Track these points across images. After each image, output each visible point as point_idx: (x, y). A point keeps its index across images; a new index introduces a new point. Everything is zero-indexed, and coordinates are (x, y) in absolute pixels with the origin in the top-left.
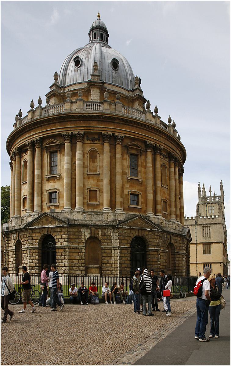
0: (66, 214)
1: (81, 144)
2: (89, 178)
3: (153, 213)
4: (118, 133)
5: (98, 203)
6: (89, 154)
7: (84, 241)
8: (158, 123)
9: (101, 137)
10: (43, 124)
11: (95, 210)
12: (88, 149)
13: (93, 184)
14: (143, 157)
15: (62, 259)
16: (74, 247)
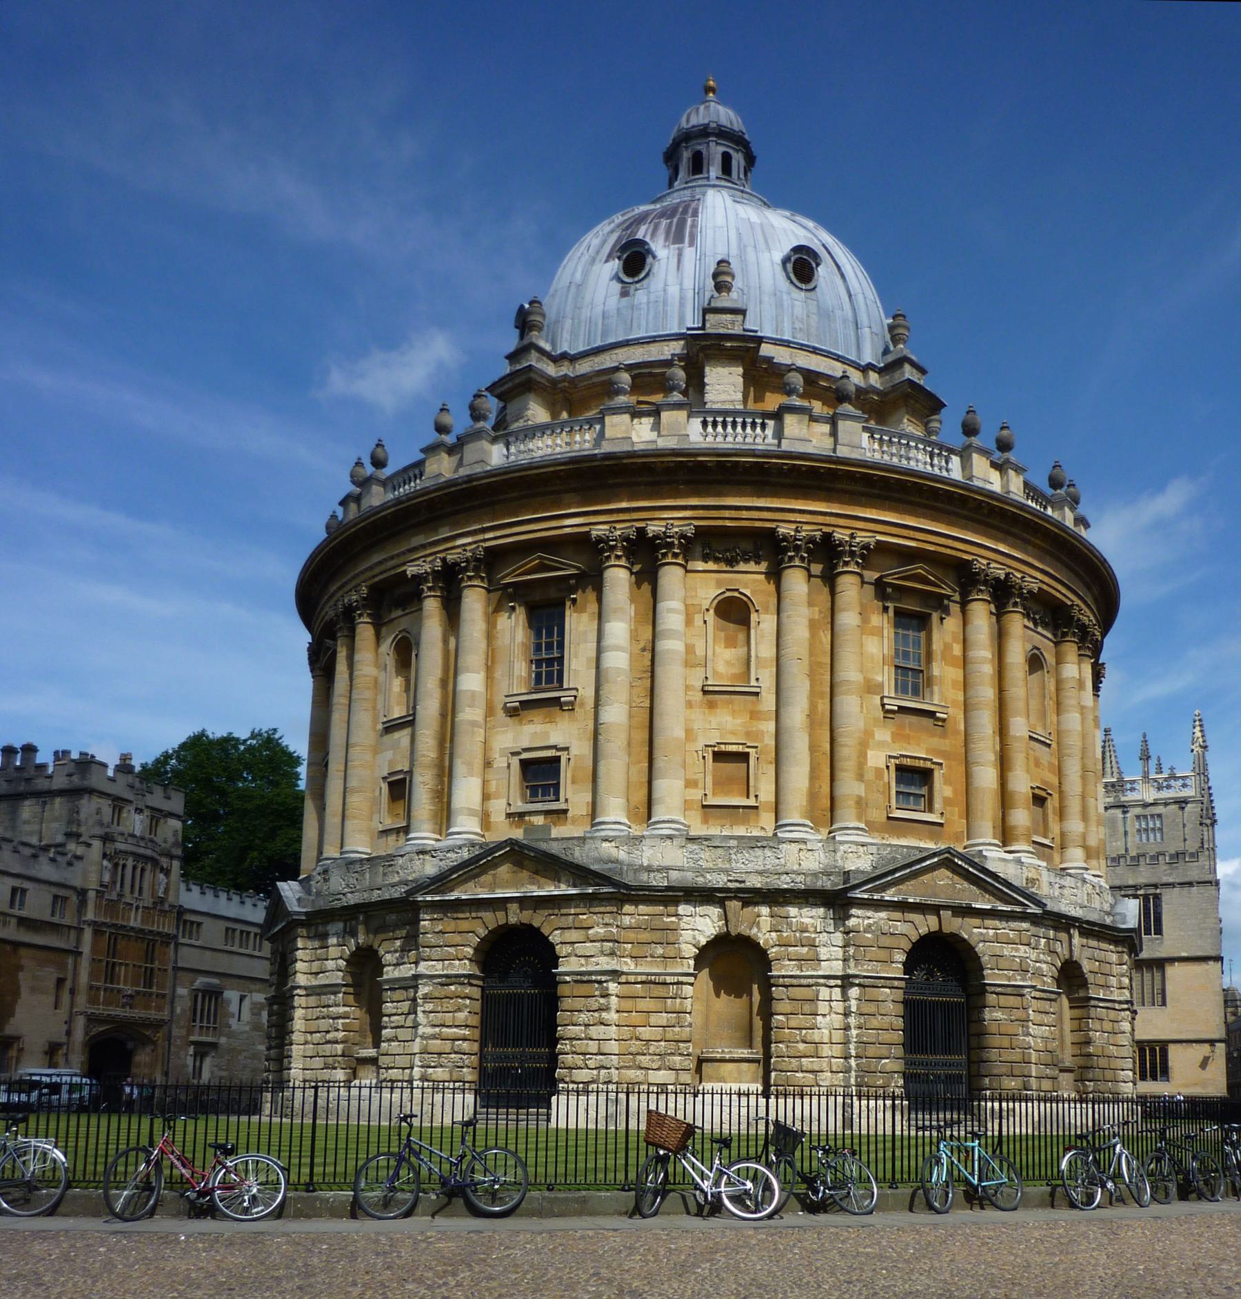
1: (679, 571)
2: (711, 706)
3: (996, 842)
4: (849, 532)
5: (751, 802)
6: (712, 611)
8: (1015, 491)
10: (502, 497)
11: (740, 831)
13: (729, 727)
14: (952, 624)
15: (587, 1025)
16: (644, 978)
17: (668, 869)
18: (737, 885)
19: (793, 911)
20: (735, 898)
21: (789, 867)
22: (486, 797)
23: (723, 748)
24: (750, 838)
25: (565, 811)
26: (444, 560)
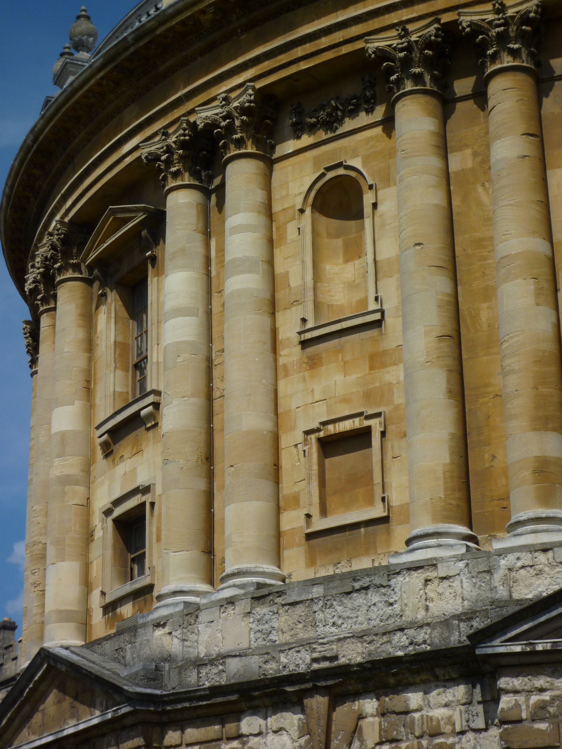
0: (159, 632)
2: (313, 363)
5: (378, 512)
6: (308, 211)
17: (224, 657)
18: (325, 665)
19: (414, 699)
20: (315, 691)
21: (409, 616)
23: (332, 429)
24: (342, 577)
25: (150, 588)
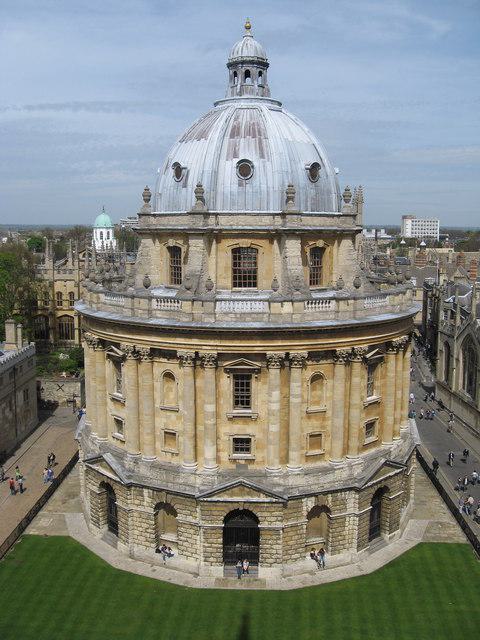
2: (309, 418)
7: (305, 514)
9: (331, 354)
12: (309, 373)
22: (218, 451)
26: (197, 353)
